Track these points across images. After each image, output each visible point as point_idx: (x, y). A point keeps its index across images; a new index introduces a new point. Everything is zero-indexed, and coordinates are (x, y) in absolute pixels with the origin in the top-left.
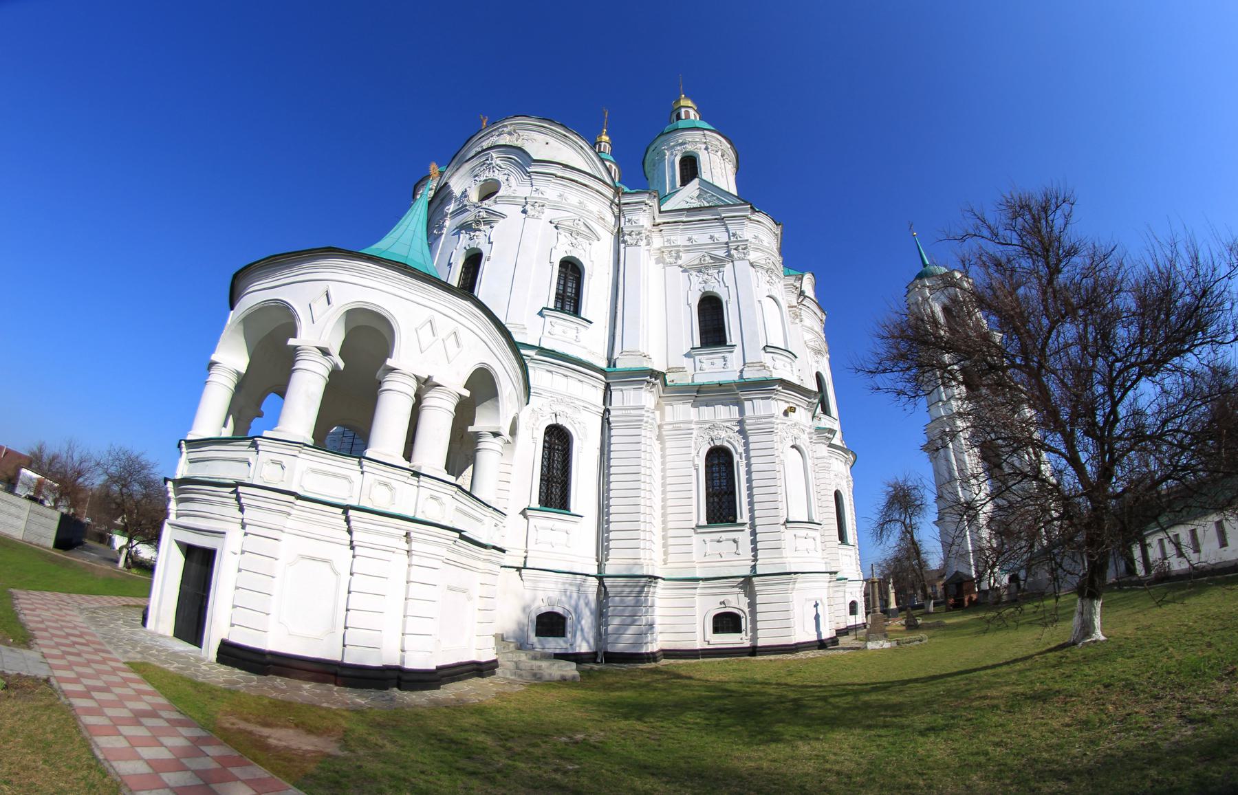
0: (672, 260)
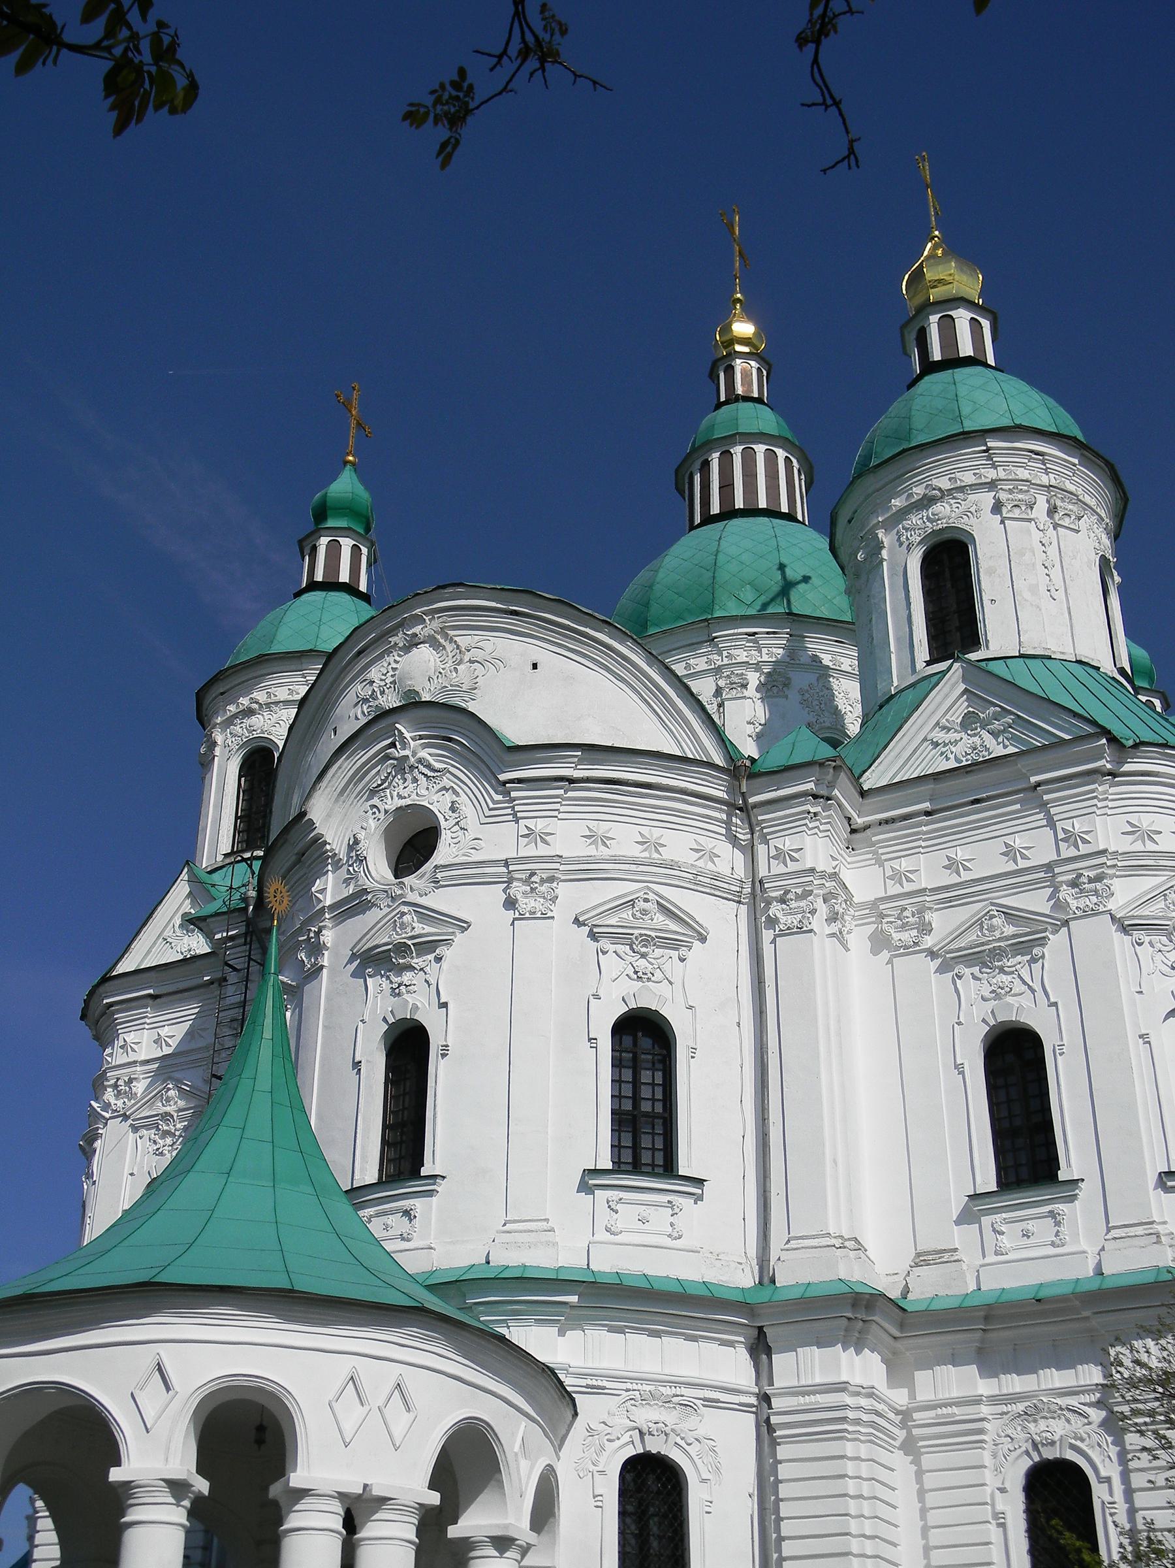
0: (907, 936)
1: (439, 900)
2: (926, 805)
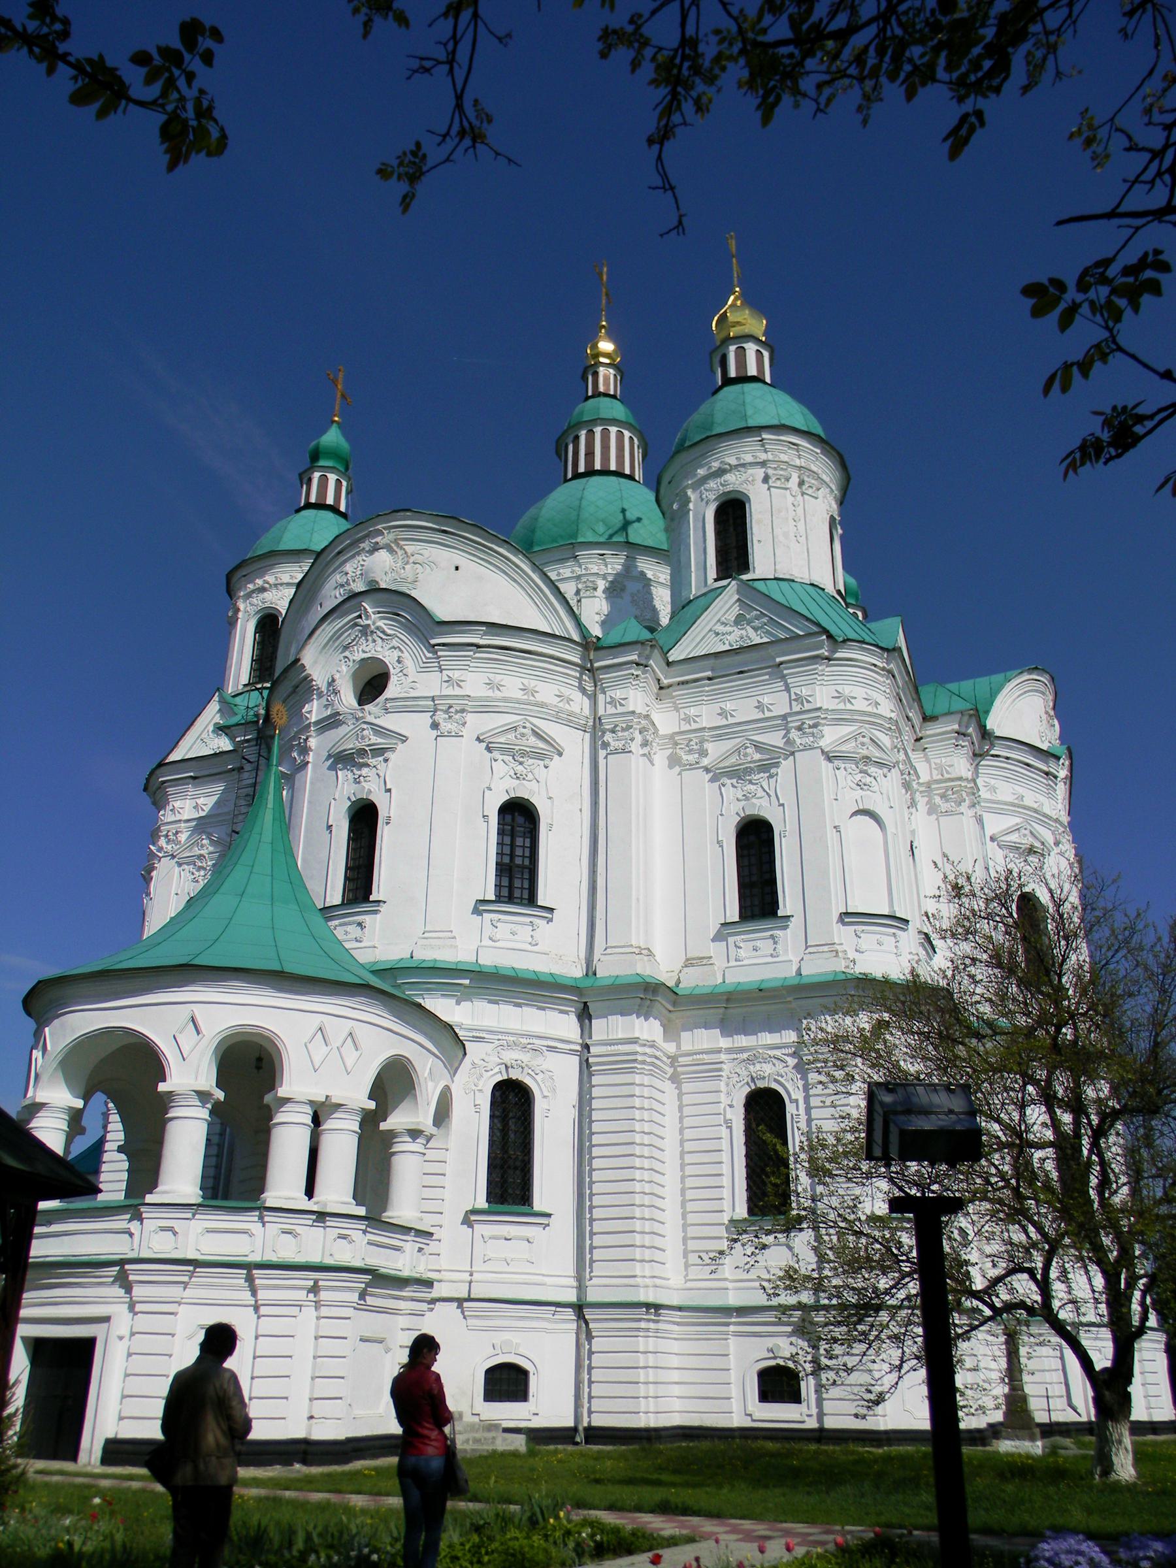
0: (692, 758)
1: (390, 722)
2: (709, 674)
